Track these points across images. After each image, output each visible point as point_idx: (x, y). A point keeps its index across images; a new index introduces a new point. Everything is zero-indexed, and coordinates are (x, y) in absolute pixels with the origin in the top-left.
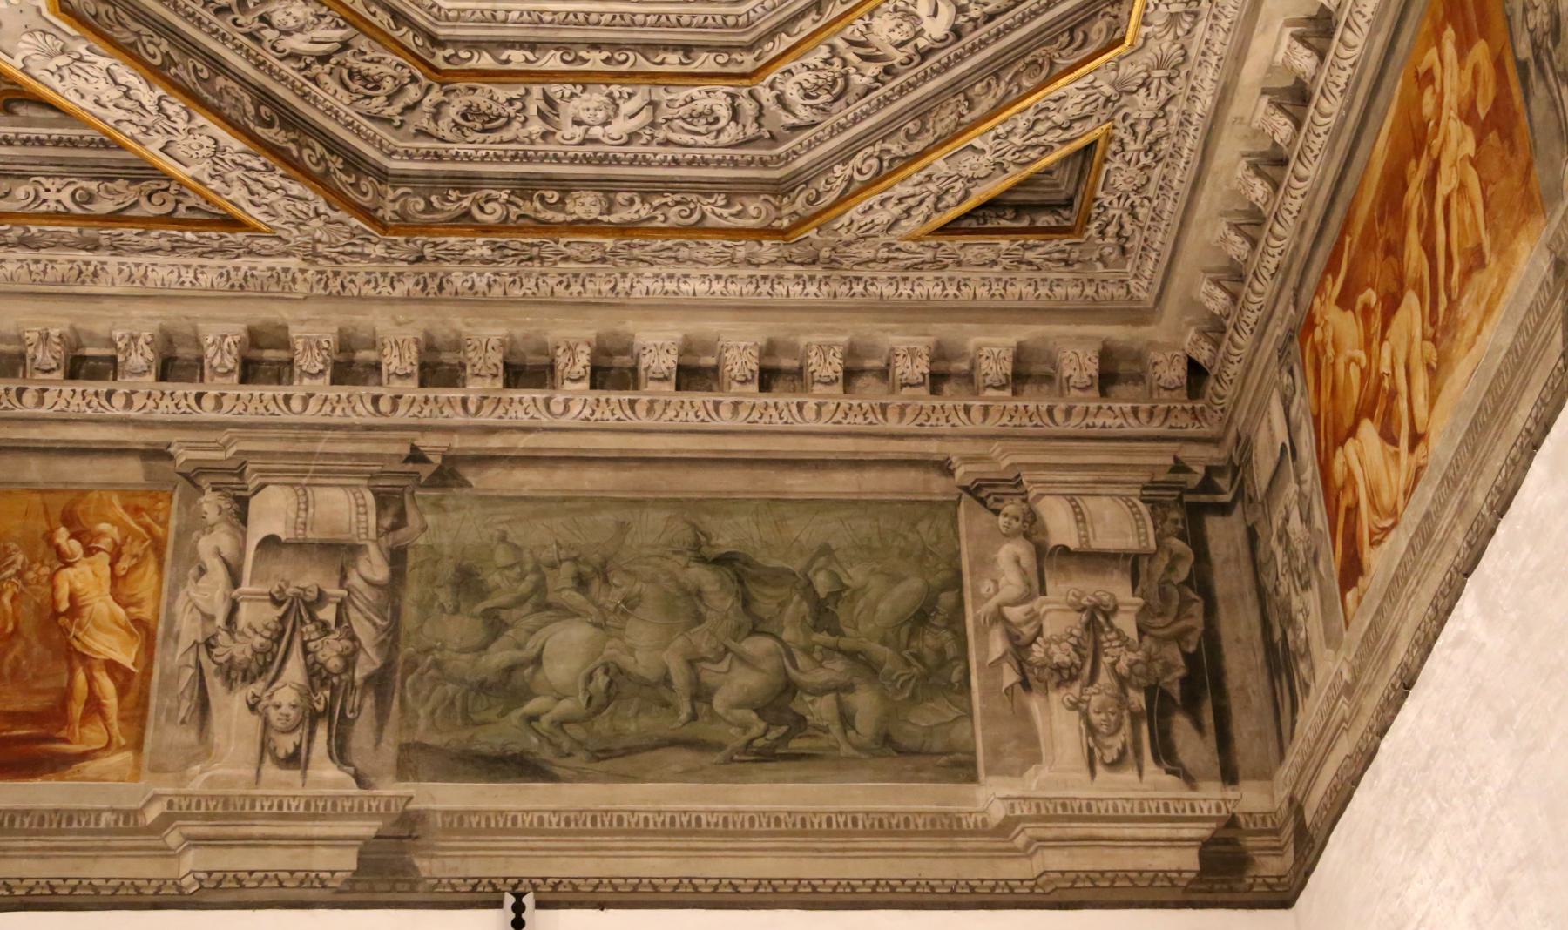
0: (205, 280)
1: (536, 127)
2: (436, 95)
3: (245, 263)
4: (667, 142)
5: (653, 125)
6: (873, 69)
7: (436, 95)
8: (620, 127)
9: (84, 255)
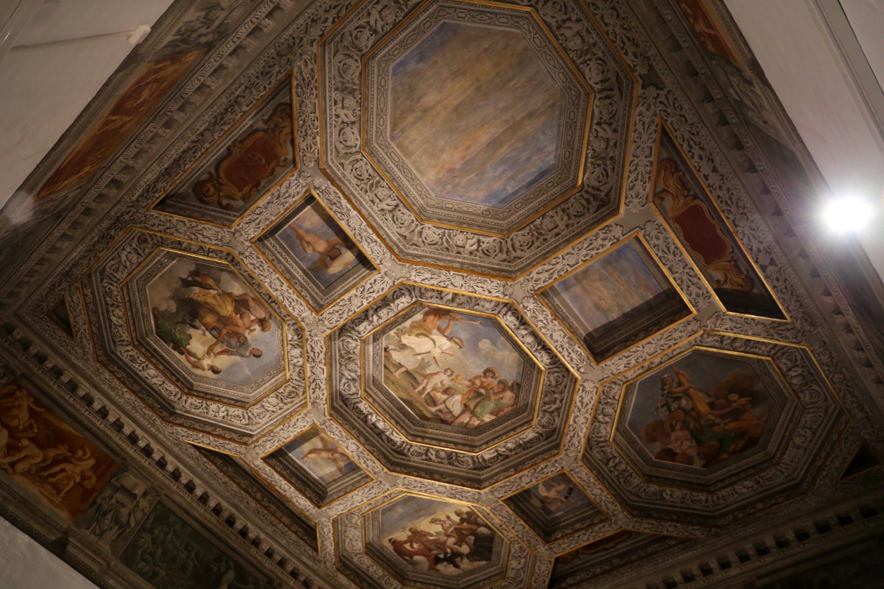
0: (142, 183)
1: (134, 245)
2: (155, 241)
3: (141, 191)
4: (113, 259)
5: (120, 262)
6: (109, 302)
7: (155, 241)
8: (124, 258)
9: (166, 166)
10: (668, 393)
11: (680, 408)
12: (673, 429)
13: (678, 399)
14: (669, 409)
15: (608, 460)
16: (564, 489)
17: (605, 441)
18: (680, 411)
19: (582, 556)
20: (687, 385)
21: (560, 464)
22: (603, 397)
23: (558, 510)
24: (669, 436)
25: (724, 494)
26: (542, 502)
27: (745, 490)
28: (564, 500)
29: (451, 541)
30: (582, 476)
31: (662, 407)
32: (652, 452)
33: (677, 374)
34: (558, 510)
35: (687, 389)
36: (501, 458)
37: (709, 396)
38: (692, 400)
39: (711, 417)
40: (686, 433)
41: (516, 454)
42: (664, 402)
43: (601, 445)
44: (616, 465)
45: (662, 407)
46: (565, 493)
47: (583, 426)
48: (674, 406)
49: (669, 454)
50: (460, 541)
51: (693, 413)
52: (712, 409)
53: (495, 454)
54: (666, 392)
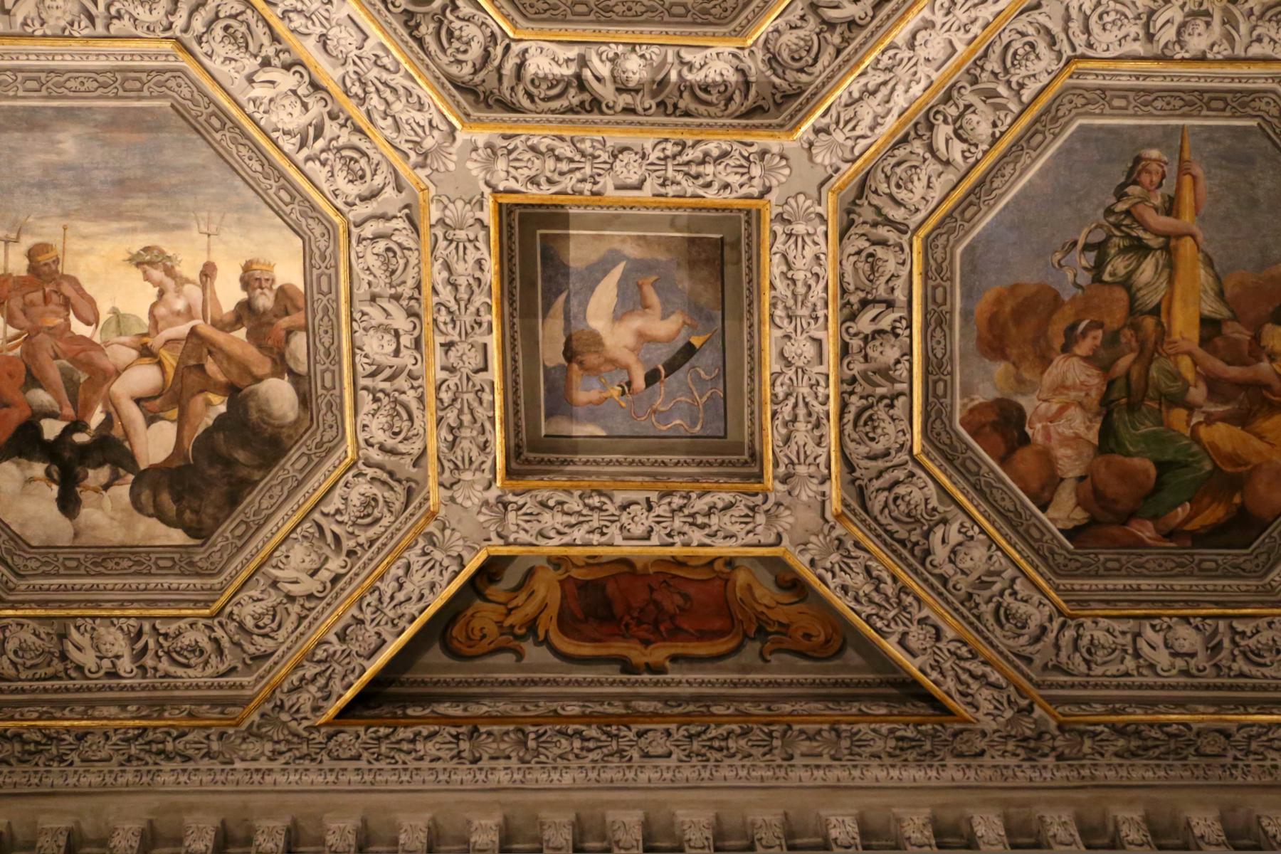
10: (1128, 213)
11: (1126, 283)
12: (1066, 349)
13: (1139, 249)
14: (1099, 266)
15: (864, 303)
16: (670, 340)
17: (901, 228)
18: (1121, 294)
19: (534, 653)
20: (1187, 219)
21: (768, 171)
22: (993, 64)
23: (594, 412)
24: (1045, 361)
25: (1100, 635)
26: (570, 353)
27: (1162, 658)
28: (639, 382)
29: (144, 378)
30: (801, 264)
31: (1087, 247)
32: (966, 393)
33: (1183, 170)
34: (594, 412)
35: (1179, 236)
36: (573, 98)
37: (1220, 294)
38: (1171, 281)
39: (1185, 364)
40: (1094, 380)
41: (629, 110)
42: (1099, 236)
43: (883, 232)
44: (881, 332)
45: (1087, 247)
46: (660, 356)
47: (923, 70)
48: (1118, 265)
49: (1005, 425)
50: (167, 400)
51: (1149, 322)
52: (1204, 342)
53: (569, 71)
54: (1121, 207)
